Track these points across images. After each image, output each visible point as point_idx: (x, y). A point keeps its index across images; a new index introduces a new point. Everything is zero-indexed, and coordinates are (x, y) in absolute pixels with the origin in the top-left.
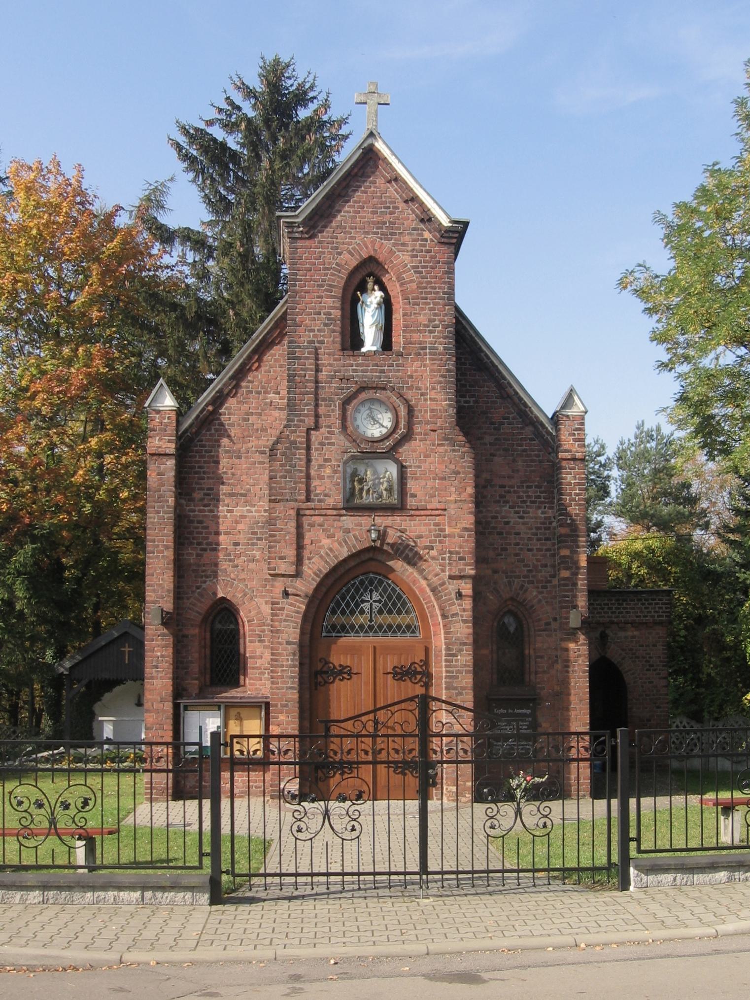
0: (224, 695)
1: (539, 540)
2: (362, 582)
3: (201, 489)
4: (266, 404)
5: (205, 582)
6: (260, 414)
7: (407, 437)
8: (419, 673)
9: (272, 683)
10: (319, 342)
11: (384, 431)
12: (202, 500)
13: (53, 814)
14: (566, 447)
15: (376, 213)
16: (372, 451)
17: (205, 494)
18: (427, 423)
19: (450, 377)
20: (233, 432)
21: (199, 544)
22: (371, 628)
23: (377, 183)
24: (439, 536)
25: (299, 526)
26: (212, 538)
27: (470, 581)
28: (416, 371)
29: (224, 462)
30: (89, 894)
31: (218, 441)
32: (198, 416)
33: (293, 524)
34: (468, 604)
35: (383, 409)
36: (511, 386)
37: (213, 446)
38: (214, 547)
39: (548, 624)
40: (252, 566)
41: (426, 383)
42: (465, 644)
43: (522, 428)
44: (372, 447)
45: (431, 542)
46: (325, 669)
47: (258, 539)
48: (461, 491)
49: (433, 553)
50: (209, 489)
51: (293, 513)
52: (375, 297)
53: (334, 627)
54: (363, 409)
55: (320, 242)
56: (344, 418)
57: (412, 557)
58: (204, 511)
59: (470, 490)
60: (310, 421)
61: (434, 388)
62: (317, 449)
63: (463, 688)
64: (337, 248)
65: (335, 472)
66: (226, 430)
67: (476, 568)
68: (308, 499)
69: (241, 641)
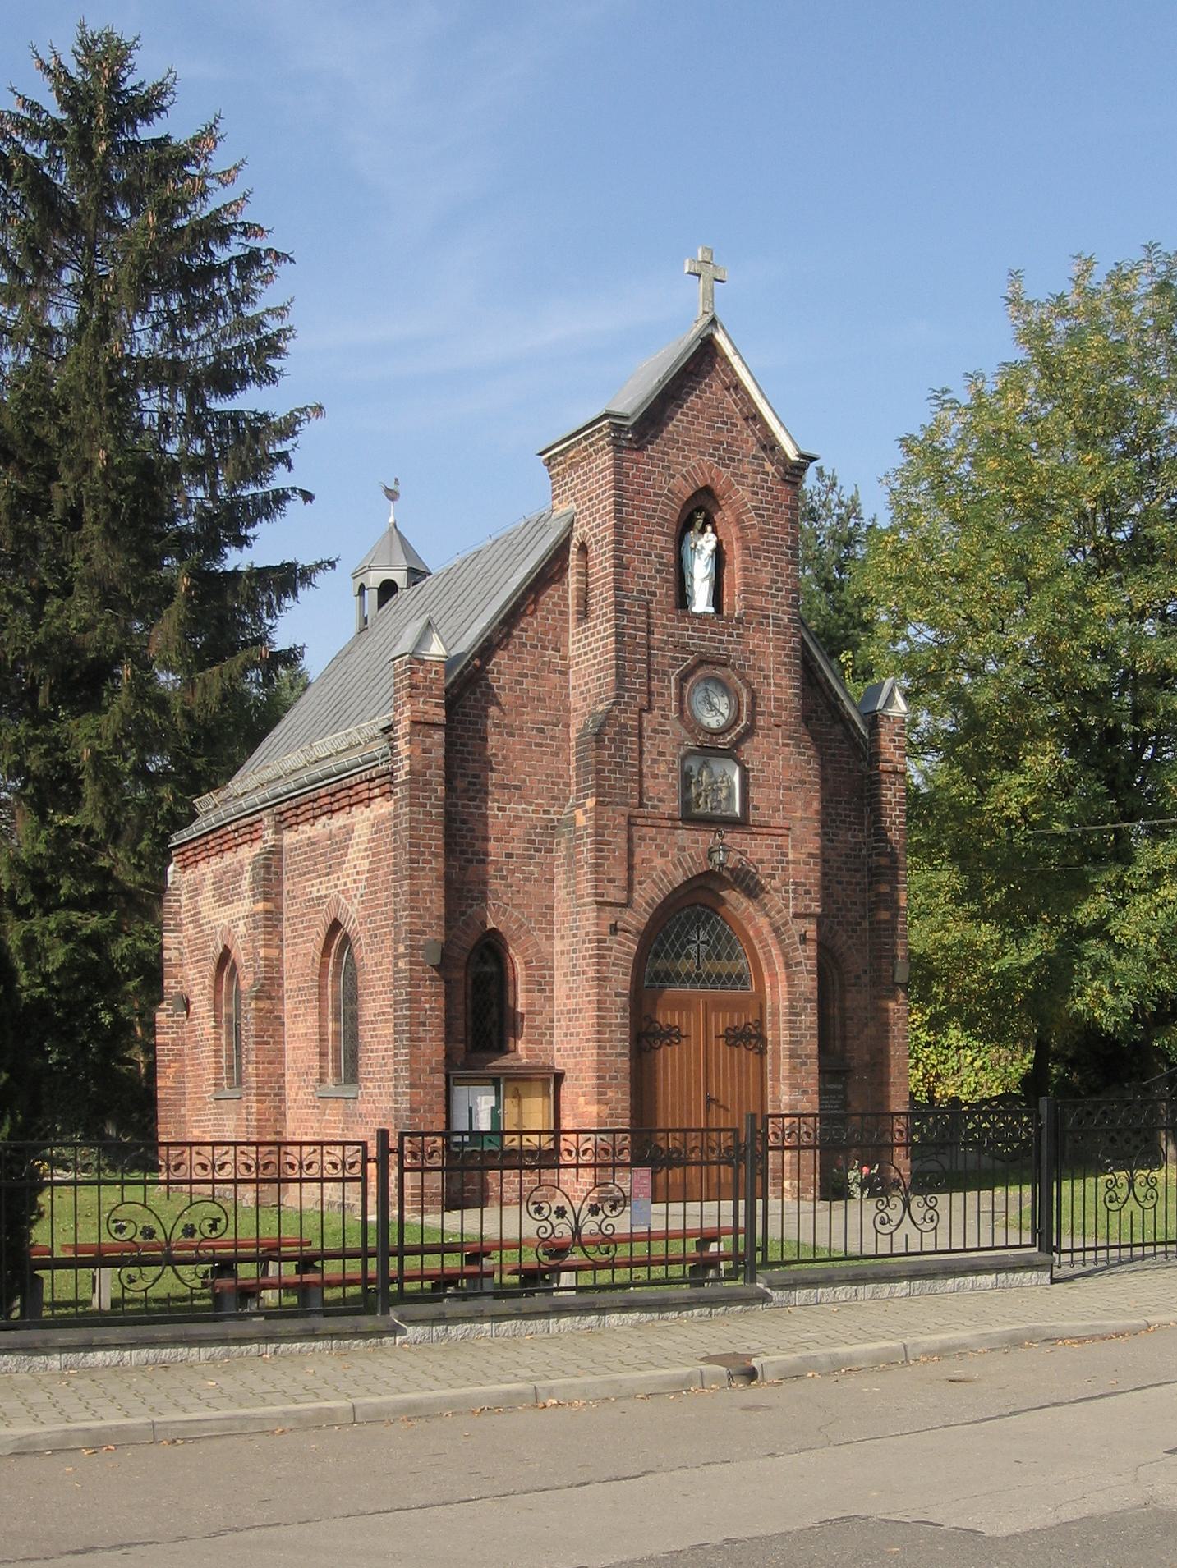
0: (494, 1064)
1: (848, 870)
2: (688, 917)
3: (464, 775)
4: (544, 663)
5: (471, 906)
6: (536, 677)
7: (749, 732)
8: (754, 1036)
9: (599, 1047)
10: (651, 593)
11: (722, 721)
12: (466, 791)
13: (577, 1220)
14: (887, 756)
15: (712, 428)
16: (713, 747)
17: (470, 783)
18: (771, 715)
19: (796, 657)
20: (503, 698)
21: (463, 852)
22: (698, 976)
23: (712, 389)
24: (781, 861)
25: (630, 839)
26: (478, 844)
27: (814, 921)
28: (758, 646)
29: (493, 740)
30: (950, 1282)
31: (485, 709)
32: (461, 672)
33: (623, 834)
34: (812, 949)
35: (719, 691)
36: (822, 671)
37: (479, 716)
38: (482, 859)
39: (858, 977)
40: (529, 887)
41: (770, 663)
42: (810, 1001)
43: (831, 726)
44: (711, 741)
45: (773, 869)
46: (651, 1030)
47: (537, 850)
48: (807, 805)
49: (776, 883)
50: (475, 776)
51: (623, 821)
52: (707, 543)
53: (657, 974)
54: (698, 689)
55: (649, 457)
56: (681, 699)
57: (753, 890)
58: (468, 807)
59: (816, 805)
60: (641, 699)
61: (779, 671)
62: (650, 738)
63: (808, 1056)
64: (669, 468)
65: (671, 770)
66: (495, 695)
67: (824, 905)
68: (641, 805)
69: (511, 988)
